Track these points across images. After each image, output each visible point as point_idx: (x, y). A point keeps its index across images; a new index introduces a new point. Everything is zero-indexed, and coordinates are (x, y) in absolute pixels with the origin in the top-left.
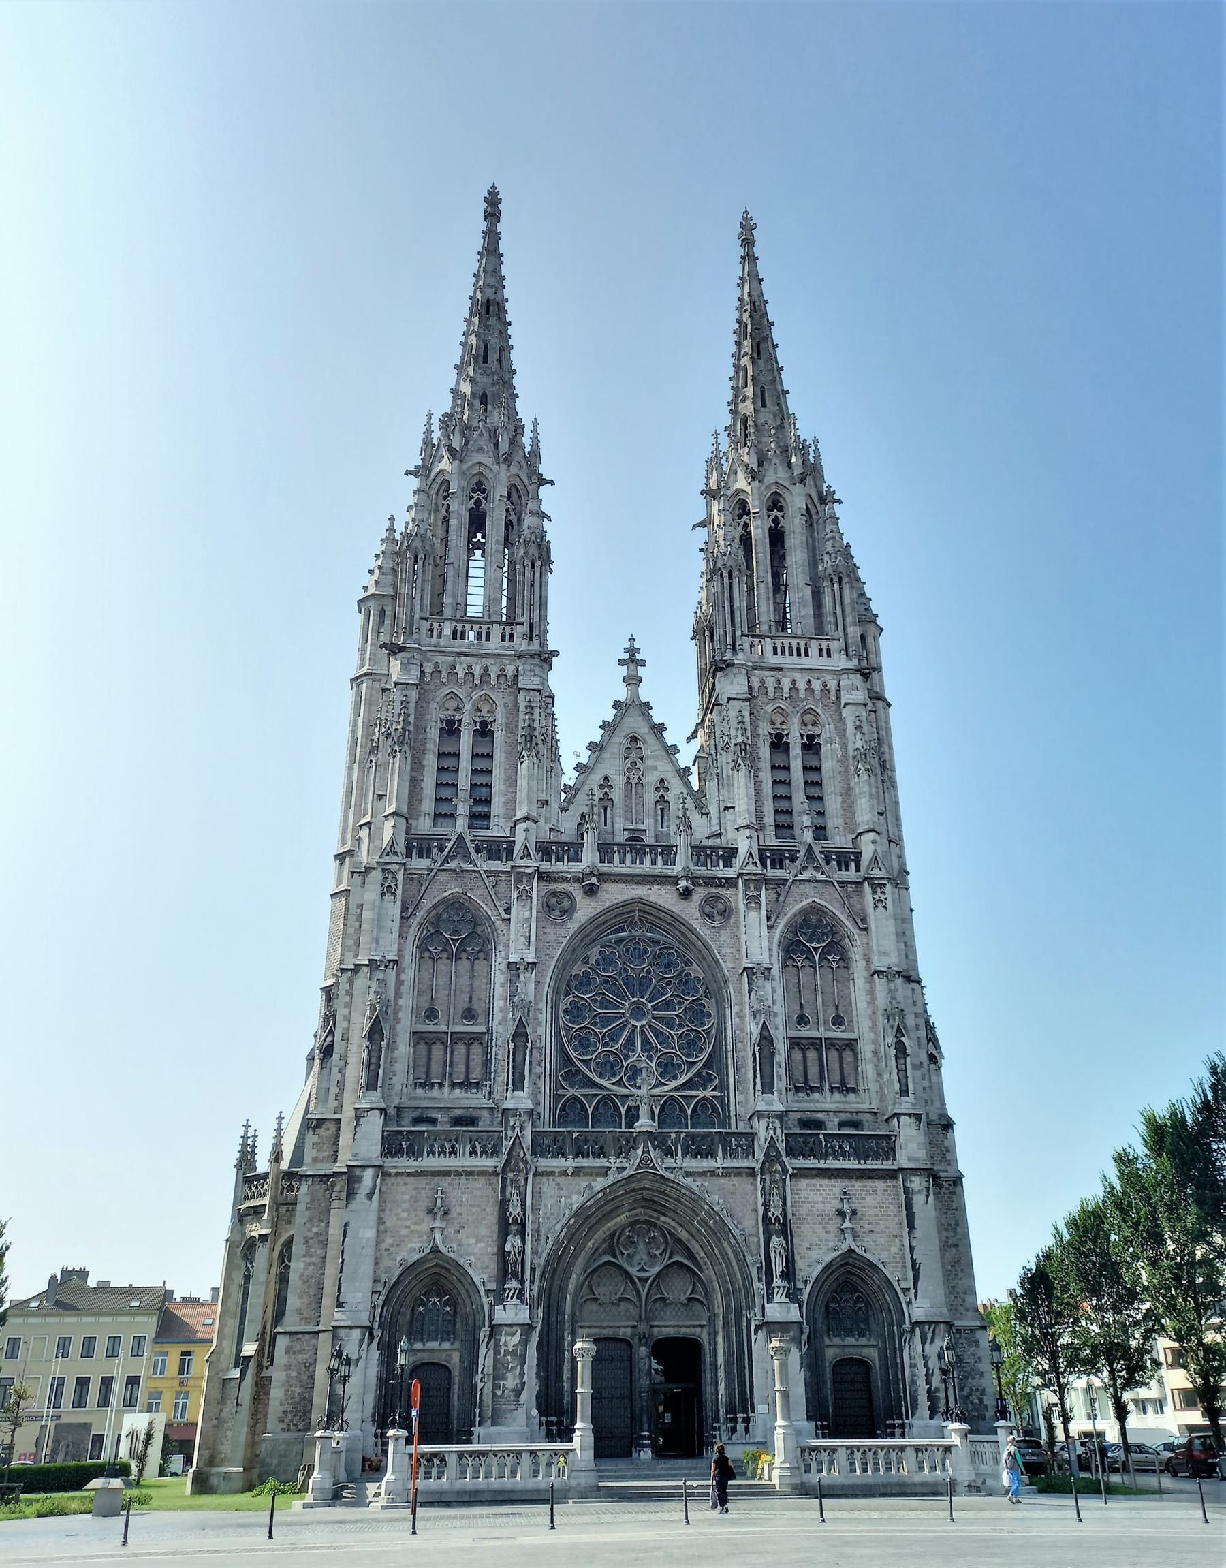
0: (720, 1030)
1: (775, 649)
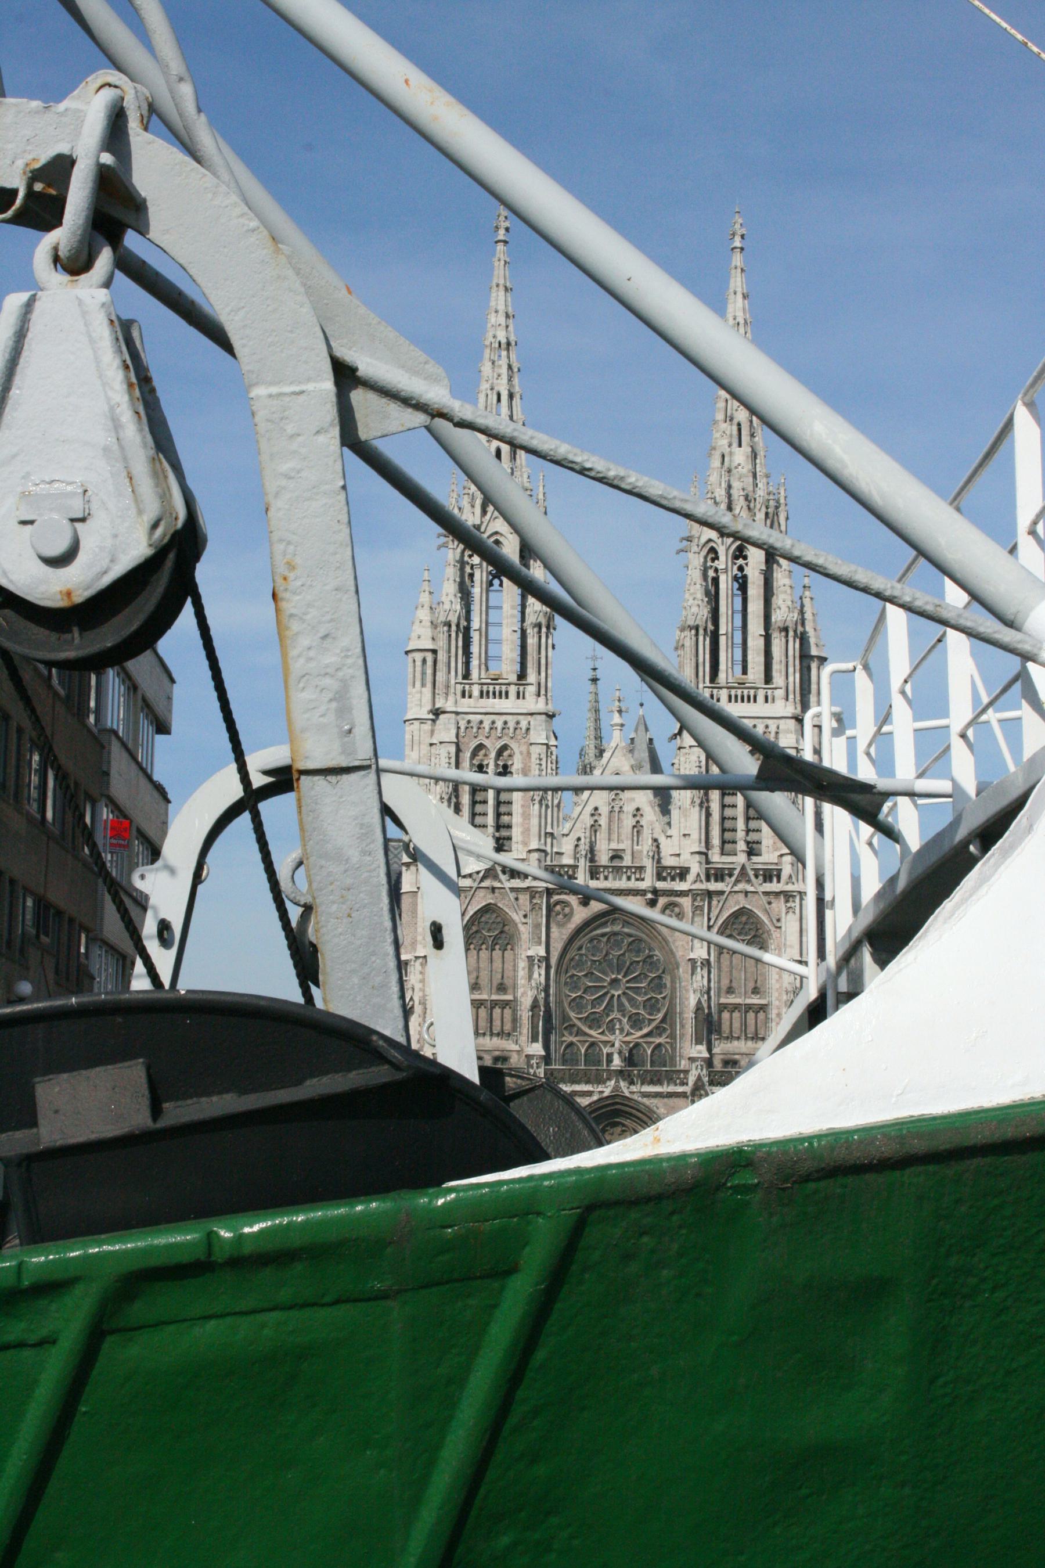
0: (673, 998)
1: (730, 697)
